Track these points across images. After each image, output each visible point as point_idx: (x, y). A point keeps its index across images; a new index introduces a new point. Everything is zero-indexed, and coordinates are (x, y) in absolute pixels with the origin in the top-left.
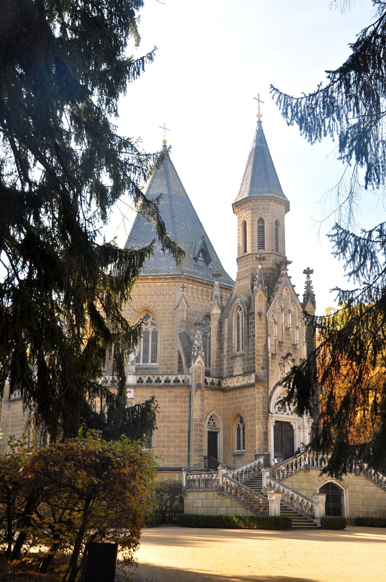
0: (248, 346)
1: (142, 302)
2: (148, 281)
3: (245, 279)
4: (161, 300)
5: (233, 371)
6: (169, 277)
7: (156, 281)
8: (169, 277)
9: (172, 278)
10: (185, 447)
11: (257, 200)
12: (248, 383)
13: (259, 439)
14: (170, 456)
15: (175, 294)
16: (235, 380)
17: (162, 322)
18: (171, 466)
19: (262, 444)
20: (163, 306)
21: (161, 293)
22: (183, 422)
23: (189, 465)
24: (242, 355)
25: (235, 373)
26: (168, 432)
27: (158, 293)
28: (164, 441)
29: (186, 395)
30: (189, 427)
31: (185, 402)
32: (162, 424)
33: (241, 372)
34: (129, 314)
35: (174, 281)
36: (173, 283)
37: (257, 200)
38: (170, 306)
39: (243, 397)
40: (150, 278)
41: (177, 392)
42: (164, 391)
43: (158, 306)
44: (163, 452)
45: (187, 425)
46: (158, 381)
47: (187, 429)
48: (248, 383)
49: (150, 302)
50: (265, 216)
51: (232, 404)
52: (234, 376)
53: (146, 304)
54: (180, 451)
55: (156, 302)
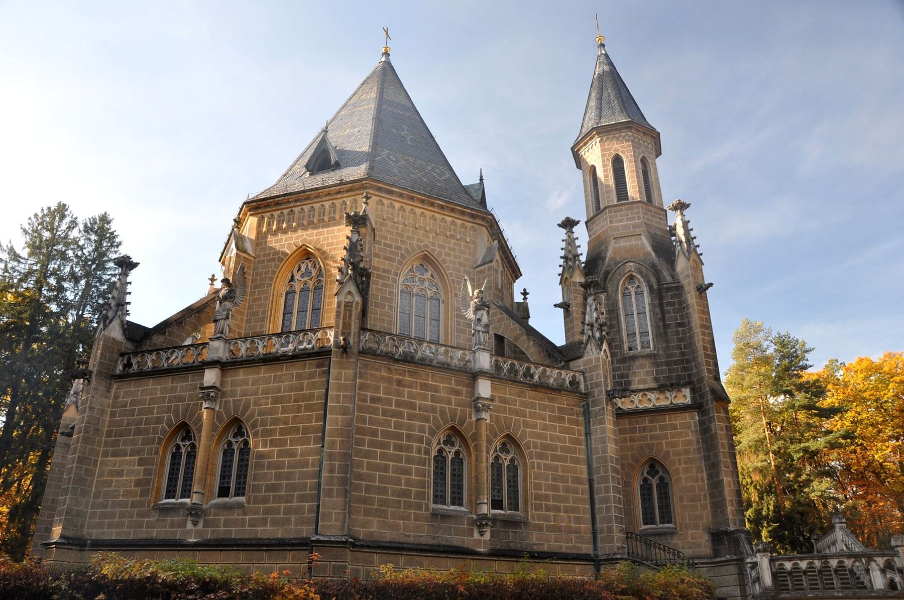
0: (667, 341)
1: (420, 240)
2: (431, 208)
3: (633, 238)
4: (452, 245)
5: (629, 383)
6: (469, 211)
7: (446, 213)
8: (469, 211)
9: (473, 216)
10: (584, 513)
11: (639, 131)
12: (672, 403)
13: (731, 501)
14: (558, 529)
15: (475, 243)
16: (636, 398)
17: (454, 283)
18: (564, 550)
19: (737, 512)
20: (455, 257)
21: (450, 235)
22: (577, 461)
23: (595, 549)
24: (649, 356)
25: (634, 387)
26: (554, 480)
27: (448, 234)
28: (547, 498)
29: (578, 409)
30: (590, 473)
31: (577, 423)
32: (542, 462)
33: (653, 385)
34: (397, 254)
35: (474, 221)
36: (471, 225)
37: (639, 131)
38: (466, 259)
39: (662, 428)
40: (438, 205)
41: (564, 401)
42: (540, 395)
43: (448, 255)
44: (547, 519)
45: (584, 467)
46: (528, 374)
47: (585, 476)
48: (672, 403)
49: (434, 244)
50: (649, 157)
51: (632, 440)
52: (635, 391)
53: (426, 246)
54: (578, 520)
55: (443, 247)
